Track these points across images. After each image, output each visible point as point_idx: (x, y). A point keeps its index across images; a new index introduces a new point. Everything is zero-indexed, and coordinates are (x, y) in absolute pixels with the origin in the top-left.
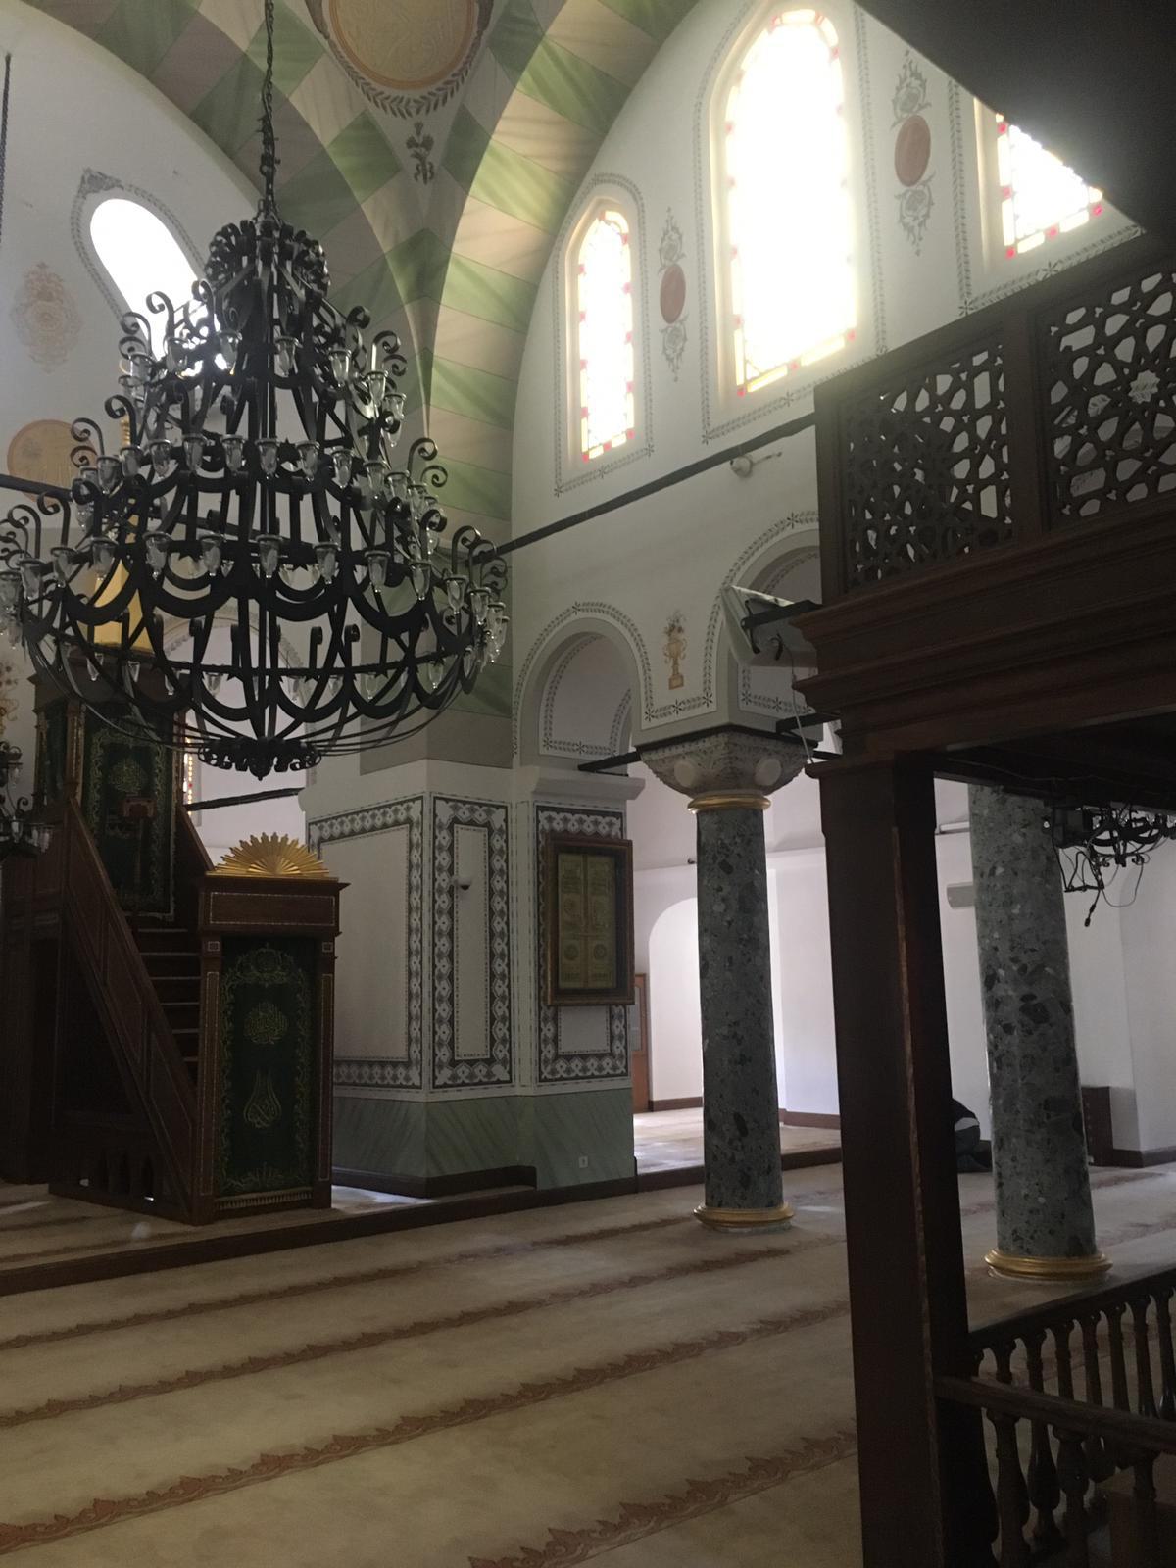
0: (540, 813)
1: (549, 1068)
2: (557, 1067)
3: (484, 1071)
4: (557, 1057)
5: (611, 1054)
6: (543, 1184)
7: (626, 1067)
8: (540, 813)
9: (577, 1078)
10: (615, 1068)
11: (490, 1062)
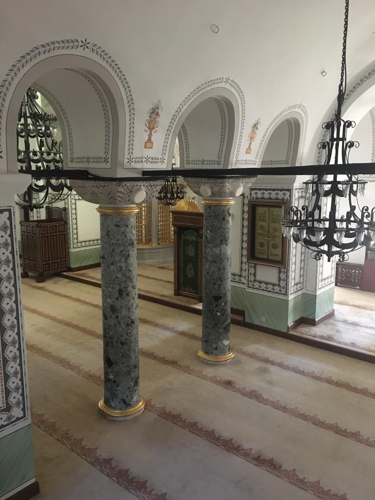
1: (252, 284)
2: (255, 284)
4: (255, 281)
5: (279, 285)
6: (247, 320)
7: (286, 292)
9: (263, 290)
10: (280, 291)
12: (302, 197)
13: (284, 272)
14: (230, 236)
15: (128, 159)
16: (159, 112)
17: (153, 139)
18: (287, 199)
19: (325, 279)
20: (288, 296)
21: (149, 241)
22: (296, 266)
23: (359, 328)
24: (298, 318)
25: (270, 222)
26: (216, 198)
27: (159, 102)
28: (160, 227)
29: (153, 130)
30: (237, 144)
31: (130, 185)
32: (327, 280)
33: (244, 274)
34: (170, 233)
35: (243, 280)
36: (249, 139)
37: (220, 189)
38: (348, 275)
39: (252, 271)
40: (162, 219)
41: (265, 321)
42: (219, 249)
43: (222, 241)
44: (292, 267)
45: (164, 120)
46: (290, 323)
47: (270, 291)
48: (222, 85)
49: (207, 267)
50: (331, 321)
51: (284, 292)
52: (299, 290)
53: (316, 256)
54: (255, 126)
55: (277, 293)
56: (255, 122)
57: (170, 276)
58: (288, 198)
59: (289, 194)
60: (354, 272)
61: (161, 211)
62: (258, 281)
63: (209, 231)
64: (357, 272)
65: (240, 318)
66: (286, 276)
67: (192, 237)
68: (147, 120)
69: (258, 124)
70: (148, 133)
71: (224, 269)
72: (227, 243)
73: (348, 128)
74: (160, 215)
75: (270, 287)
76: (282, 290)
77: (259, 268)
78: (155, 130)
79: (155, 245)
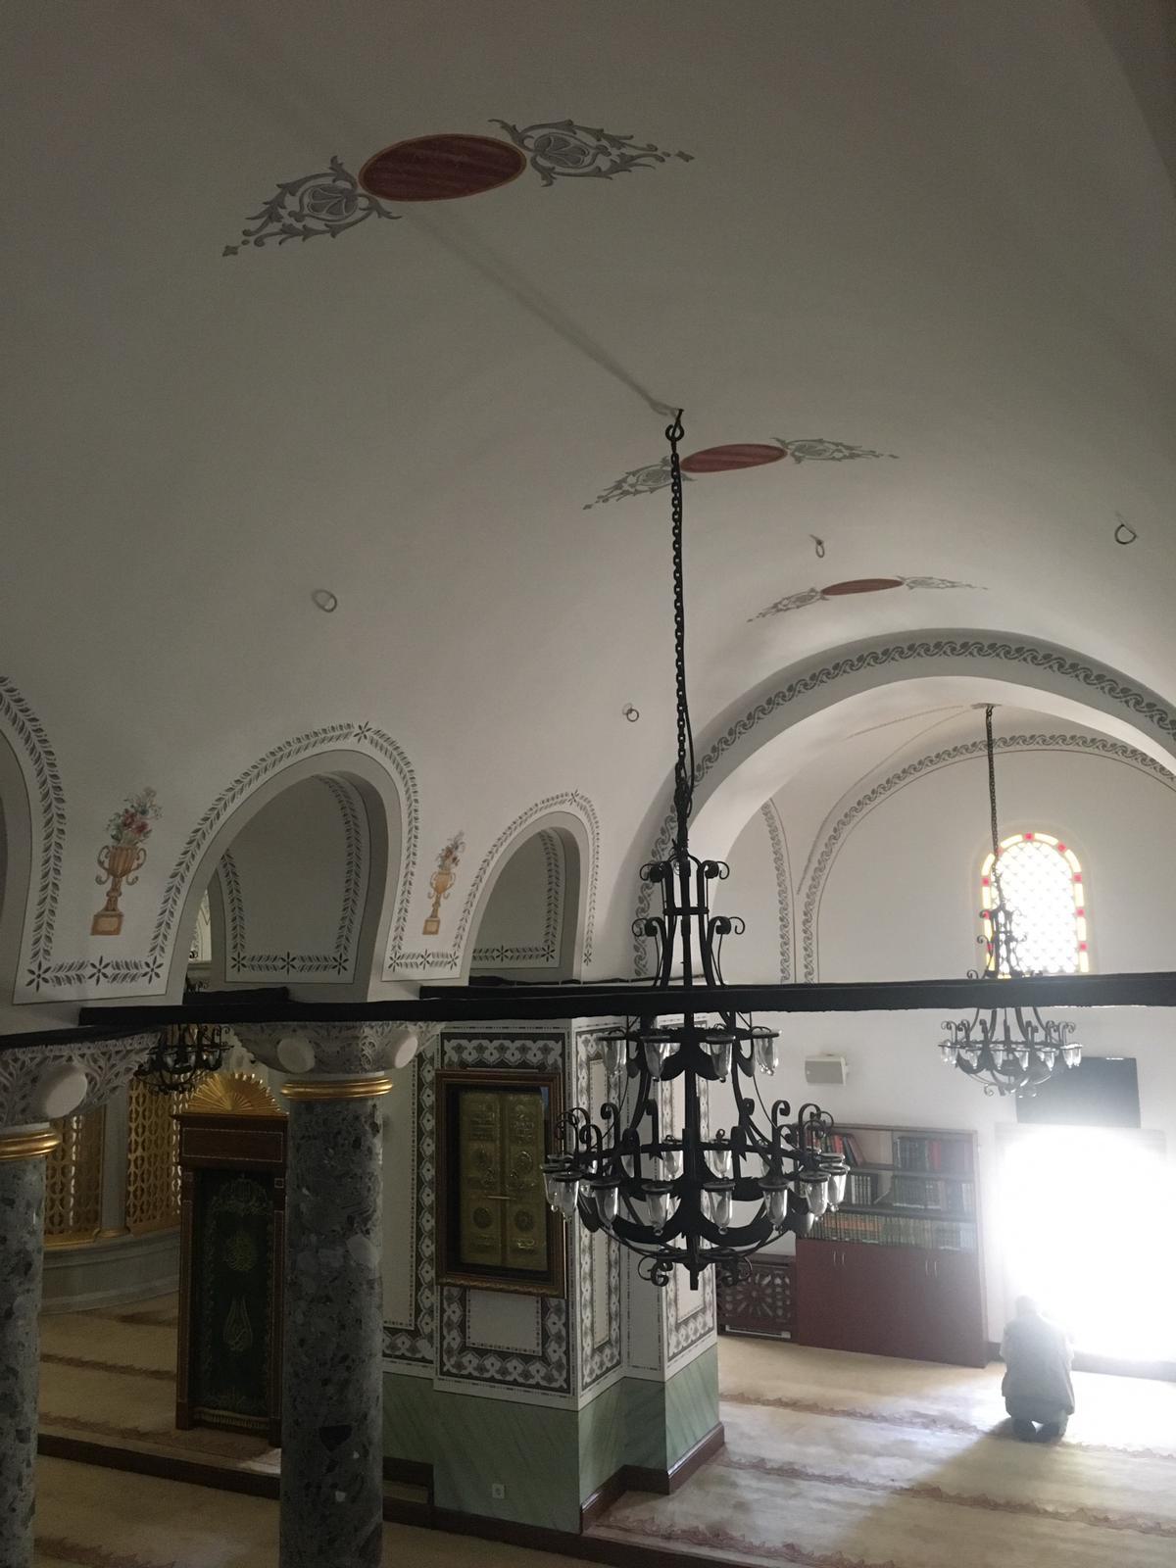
0: (445, 1041)
1: (453, 1360)
3: (408, 1343)
4: (464, 1348)
5: (544, 1359)
6: (442, 1501)
7: (567, 1380)
8: (445, 1041)
9: (492, 1379)
10: (549, 1378)
11: (415, 1334)
12: (598, 1056)
13: (558, 1311)
14: (380, 1201)
15: (33, 973)
16: (148, 822)
17: (122, 905)
18: (555, 1066)
19: (686, 1322)
20: (575, 1394)
21: (89, 1219)
22: (594, 1284)
23: (803, 1484)
24: (610, 1470)
25: (507, 1141)
26: (333, 1077)
27: (150, 793)
28: (132, 1168)
29: (124, 878)
30: (397, 906)
31: (32, 1059)
32: (691, 1325)
33: (429, 1325)
34: (169, 1185)
35: (426, 1350)
36: (432, 891)
37: (343, 1048)
38: (754, 1294)
39: (453, 1312)
40: (140, 1140)
41: (502, 1496)
42: (340, 1251)
43: (350, 1220)
44: (583, 1291)
45: (163, 847)
46: (588, 1497)
47: (515, 1383)
48: (350, 743)
49: (300, 1318)
50: (716, 1469)
51: (560, 1383)
52: (608, 1370)
53: (653, 1271)
54: (450, 855)
55: (537, 1386)
56: (449, 844)
57: (162, 1349)
58: (556, 1060)
59: (560, 1051)
60: (768, 1285)
61: (140, 1110)
62: (475, 1349)
63: (308, 1189)
64: (778, 1281)
65: (414, 1496)
66: (566, 1325)
67: (248, 1201)
68: (107, 847)
69: (457, 848)
70: (108, 886)
71: (359, 1321)
72: (368, 1226)
73: (709, 880)
74: (133, 1125)
75: (515, 1367)
76: (555, 1373)
77: (477, 1302)
78: (131, 876)
79: (111, 1234)
